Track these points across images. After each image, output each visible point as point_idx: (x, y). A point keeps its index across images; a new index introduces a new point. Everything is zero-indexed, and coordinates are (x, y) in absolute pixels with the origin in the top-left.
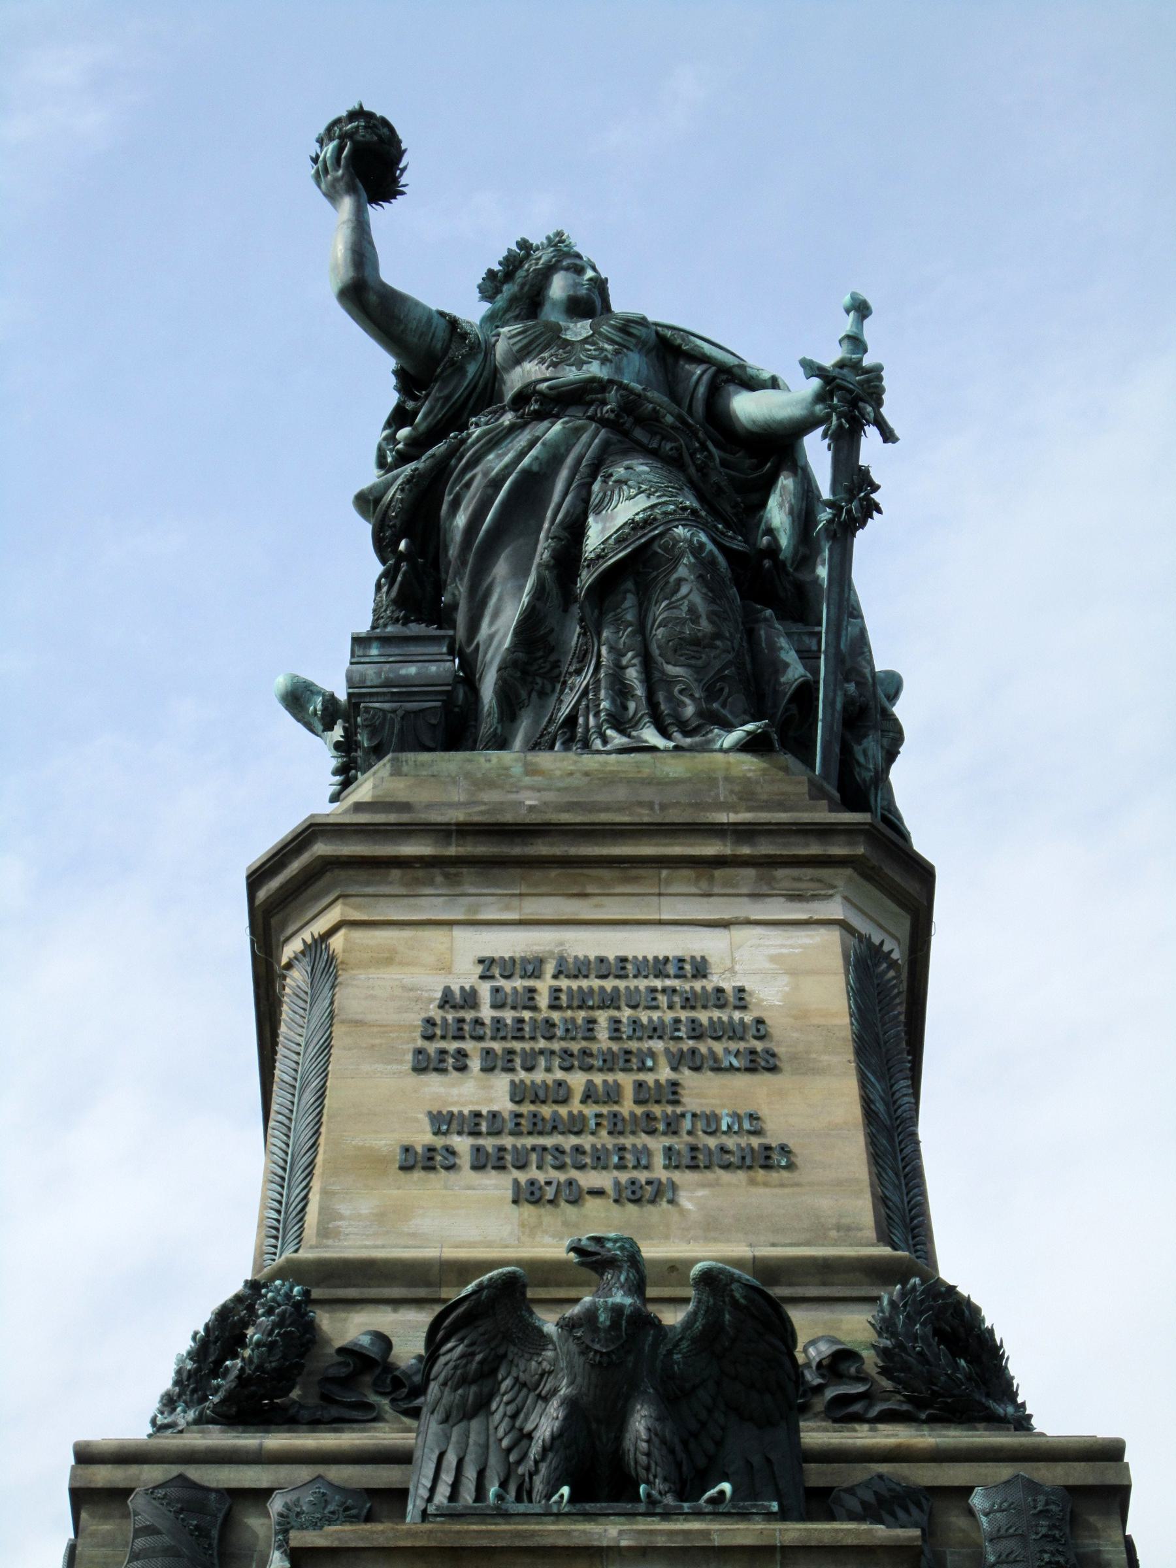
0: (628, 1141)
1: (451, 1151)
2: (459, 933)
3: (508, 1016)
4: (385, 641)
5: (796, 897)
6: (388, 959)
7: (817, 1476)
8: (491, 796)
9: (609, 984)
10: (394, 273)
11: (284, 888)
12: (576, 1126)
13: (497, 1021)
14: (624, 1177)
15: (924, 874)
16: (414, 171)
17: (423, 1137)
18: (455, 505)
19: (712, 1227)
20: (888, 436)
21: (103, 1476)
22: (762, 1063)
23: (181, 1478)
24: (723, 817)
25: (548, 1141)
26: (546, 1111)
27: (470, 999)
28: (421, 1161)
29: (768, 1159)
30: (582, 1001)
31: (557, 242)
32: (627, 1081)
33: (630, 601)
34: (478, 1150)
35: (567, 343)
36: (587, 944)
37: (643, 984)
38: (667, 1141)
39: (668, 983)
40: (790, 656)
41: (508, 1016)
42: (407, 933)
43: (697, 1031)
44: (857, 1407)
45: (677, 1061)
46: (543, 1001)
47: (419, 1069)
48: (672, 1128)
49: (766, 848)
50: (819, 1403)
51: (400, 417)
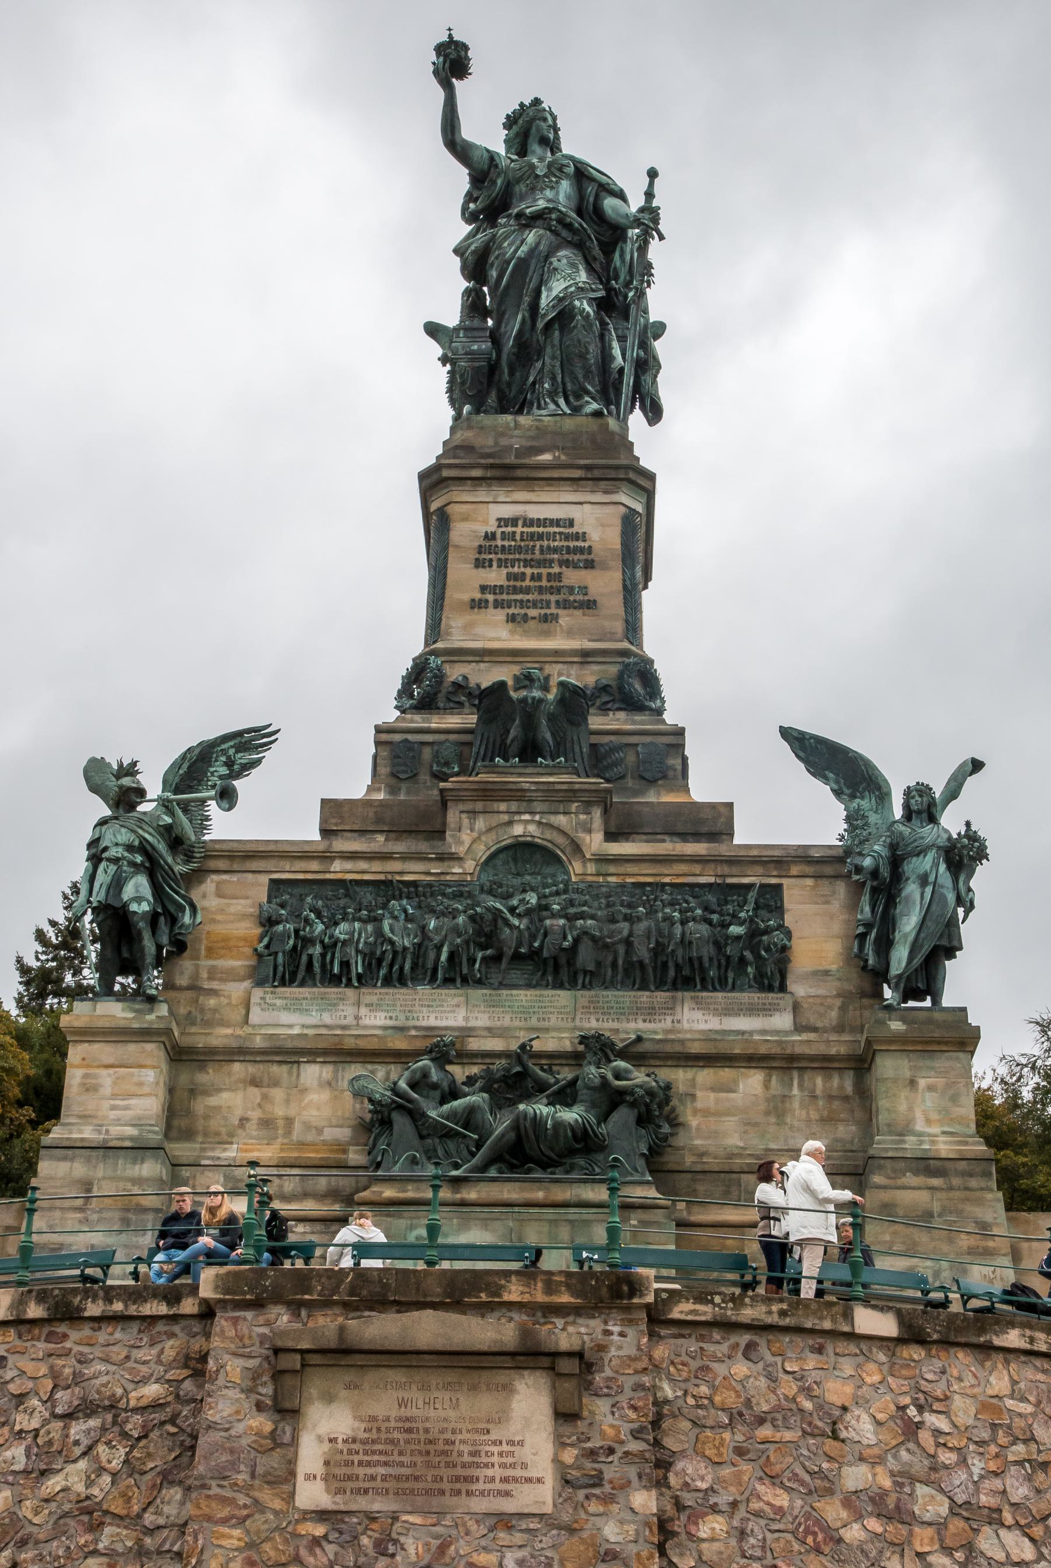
0: (544, 597)
1: (487, 601)
2: (491, 506)
3: (506, 543)
4: (466, 329)
5: (606, 492)
6: (466, 518)
7: (594, 739)
8: (504, 442)
9: (541, 530)
10: (469, 132)
11: (432, 482)
12: (527, 590)
13: (503, 546)
14: (543, 612)
15: (651, 477)
16: (474, 66)
17: (478, 596)
18: (492, 265)
19: (570, 633)
20: (661, 237)
21: (384, 737)
22: (590, 565)
23: (406, 740)
24: (582, 462)
25: (519, 597)
26: (518, 584)
27: (494, 534)
28: (478, 605)
29: (590, 605)
30: (532, 536)
31: (537, 102)
32: (544, 571)
33: (557, 333)
34: (496, 601)
35: (537, 176)
36: (535, 512)
37: (552, 530)
38: (558, 597)
39: (562, 530)
40: (617, 351)
41: (506, 543)
42: (473, 506)
43: (569, 550)
44: (609, 706)
45: (561, 563)
46: (518, 537)
47: (477, 567)
48: (558, 590)
49: (597, 473)
50: (598, 703)
51: (470, 197)
